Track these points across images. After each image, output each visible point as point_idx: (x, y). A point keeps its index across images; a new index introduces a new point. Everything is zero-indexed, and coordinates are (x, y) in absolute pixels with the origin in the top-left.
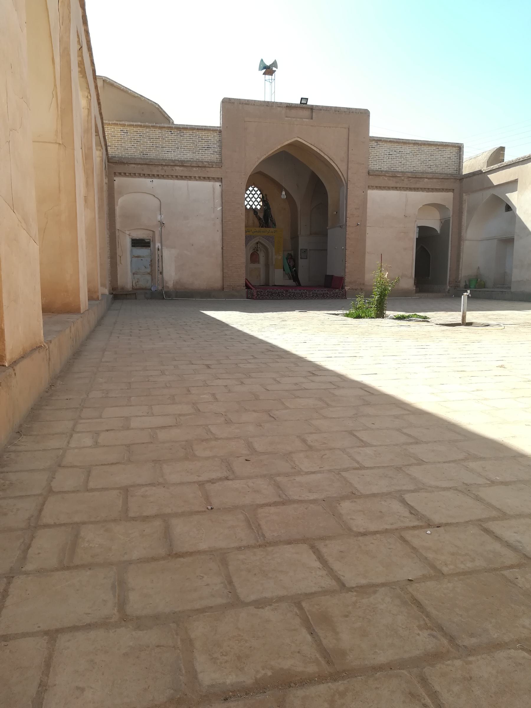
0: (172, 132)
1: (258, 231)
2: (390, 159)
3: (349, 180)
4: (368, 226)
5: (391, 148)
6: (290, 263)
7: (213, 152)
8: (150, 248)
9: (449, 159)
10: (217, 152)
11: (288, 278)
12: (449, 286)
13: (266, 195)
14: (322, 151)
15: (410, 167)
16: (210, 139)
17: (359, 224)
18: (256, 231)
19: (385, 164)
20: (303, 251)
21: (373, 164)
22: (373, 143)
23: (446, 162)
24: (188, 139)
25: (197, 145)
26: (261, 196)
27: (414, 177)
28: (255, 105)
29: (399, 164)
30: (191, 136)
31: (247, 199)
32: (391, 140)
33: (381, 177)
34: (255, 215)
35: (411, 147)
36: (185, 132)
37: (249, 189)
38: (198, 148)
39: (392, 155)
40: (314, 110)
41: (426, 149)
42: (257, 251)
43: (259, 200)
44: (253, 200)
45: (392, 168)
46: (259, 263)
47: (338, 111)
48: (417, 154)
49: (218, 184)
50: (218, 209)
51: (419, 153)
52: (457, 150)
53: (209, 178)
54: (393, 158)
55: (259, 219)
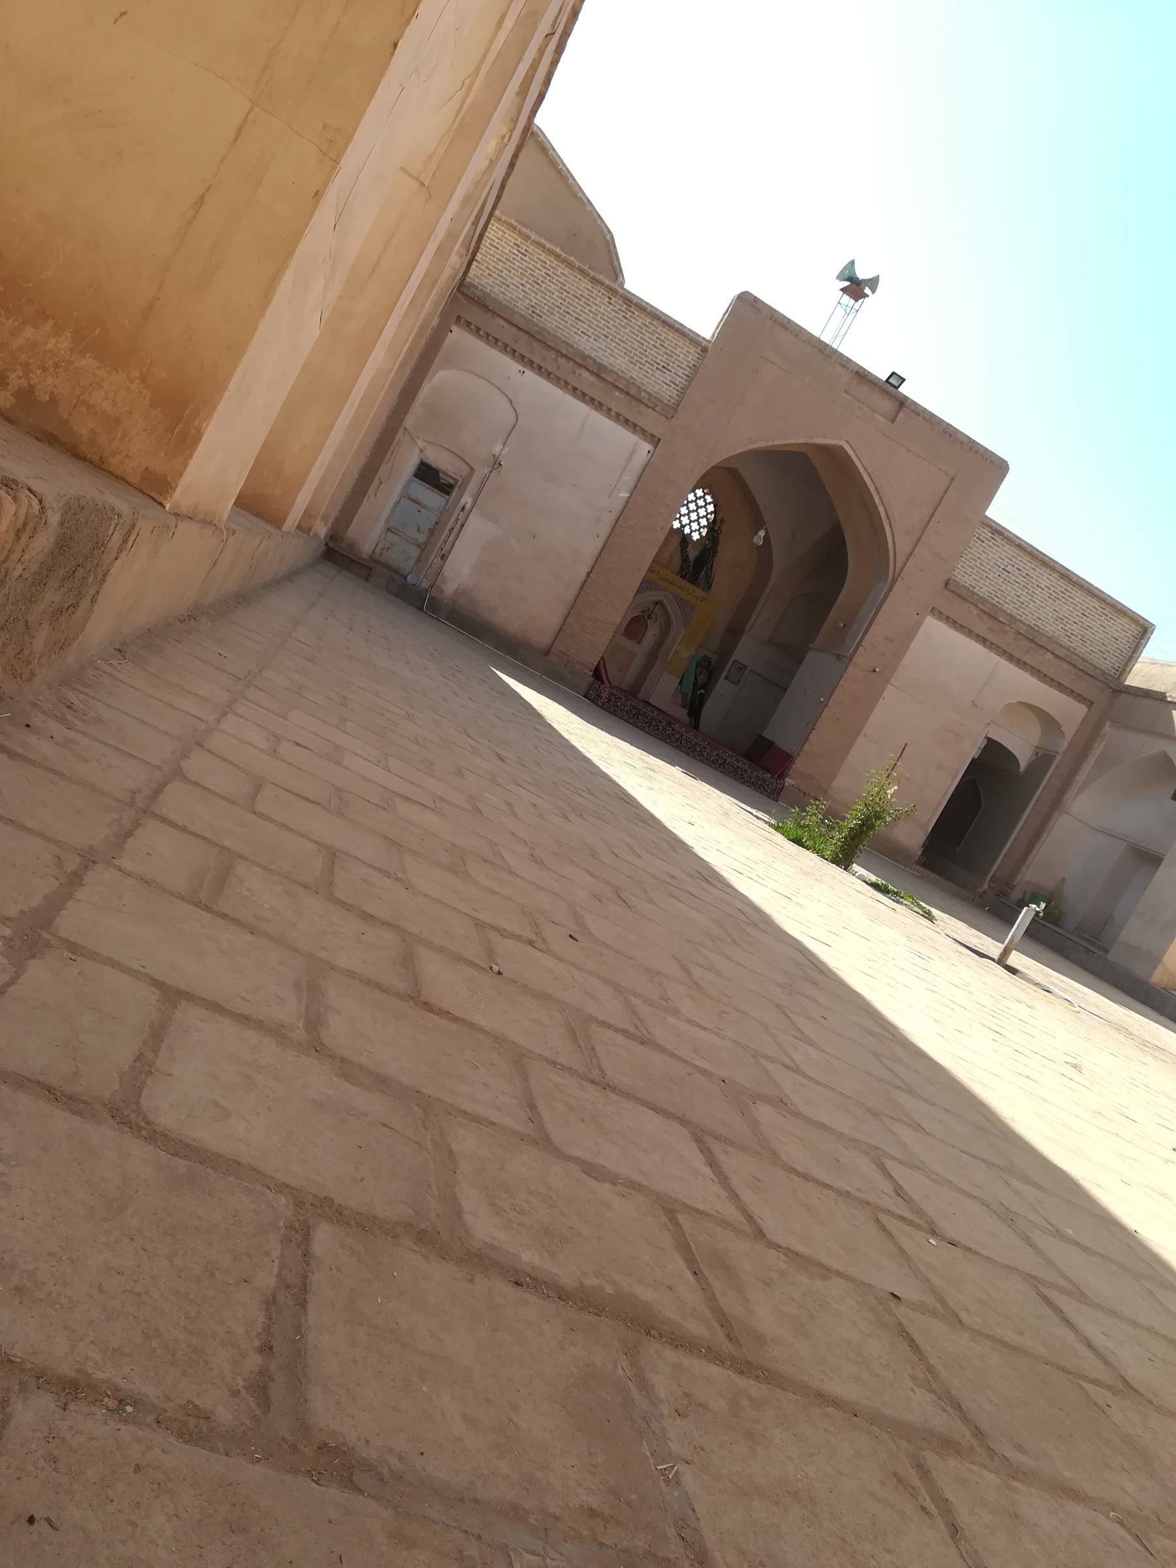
0: (612, 301)
1: (671, 581)
2: (1001, 580)
3: (902, 575)
4: (891, 684)
5: (1014, 560)
6: (700, 674)
7: (670, 381)
8: (447, 497)
9: (1114, 640)
10: (678, 386)
11: (680, 704)
12: (989, 886)
13: (722, 521)
14: (878, 493)
15: (1030, 615)
16: (677, 352)
17: (877, 670)
18: (667, 578)
19: (987, 584)
20: (738, 667)
21: (963, 570)
22: (985, 531)
23: (1105, 643)
24: (635, 331)
25: (646, 351)
27: (1031, 637)
28: (799, 336)
29: (1013, 598)
30: (645, 328)
32: (1023, 544)
33: (967, 605)
34: (681, 546)
35: (1054, 577)
36: (636, 313)
37: (697, 491)
38: (645, 359)
39: (1010, 573)
40: (906, 407)
41: (1080, 598)
42: (648, 618)
43: (704, 522)
44: (694, 516)
45: (996, 599)
46: (639, 643)
47: (950, 436)
48: (1058, 599)
49: (646, 447)
50: (620, 495)
51: (1062, 597)
52: (1138, 630)
53: (635, 425)
54: (1008, 581)
55: (685, 559)
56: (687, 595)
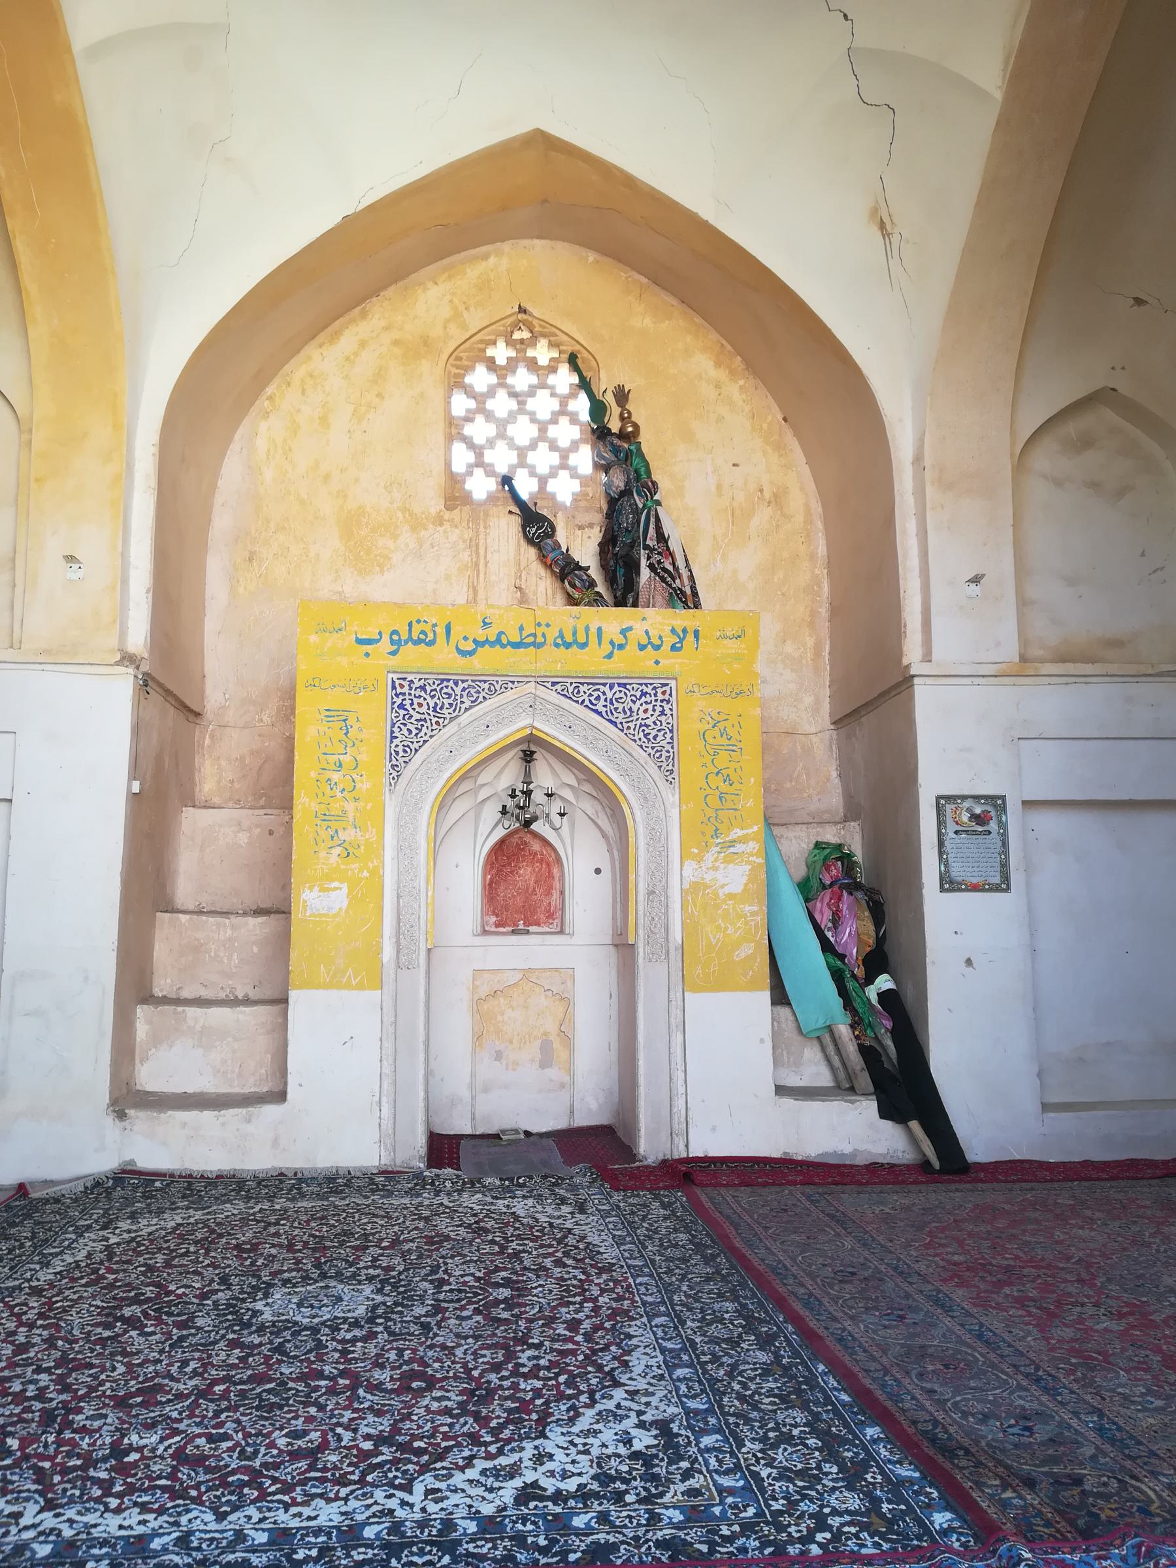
6: (836, 921)
11: (822, 1077)
13: (622, 396)
18: (492, 635)
20: (965, 817)
26: (581, 405)
31: (468, 430)
34: (530, 541)
43: (566, 433)
44: (523, 431)
56: (610, 656)
